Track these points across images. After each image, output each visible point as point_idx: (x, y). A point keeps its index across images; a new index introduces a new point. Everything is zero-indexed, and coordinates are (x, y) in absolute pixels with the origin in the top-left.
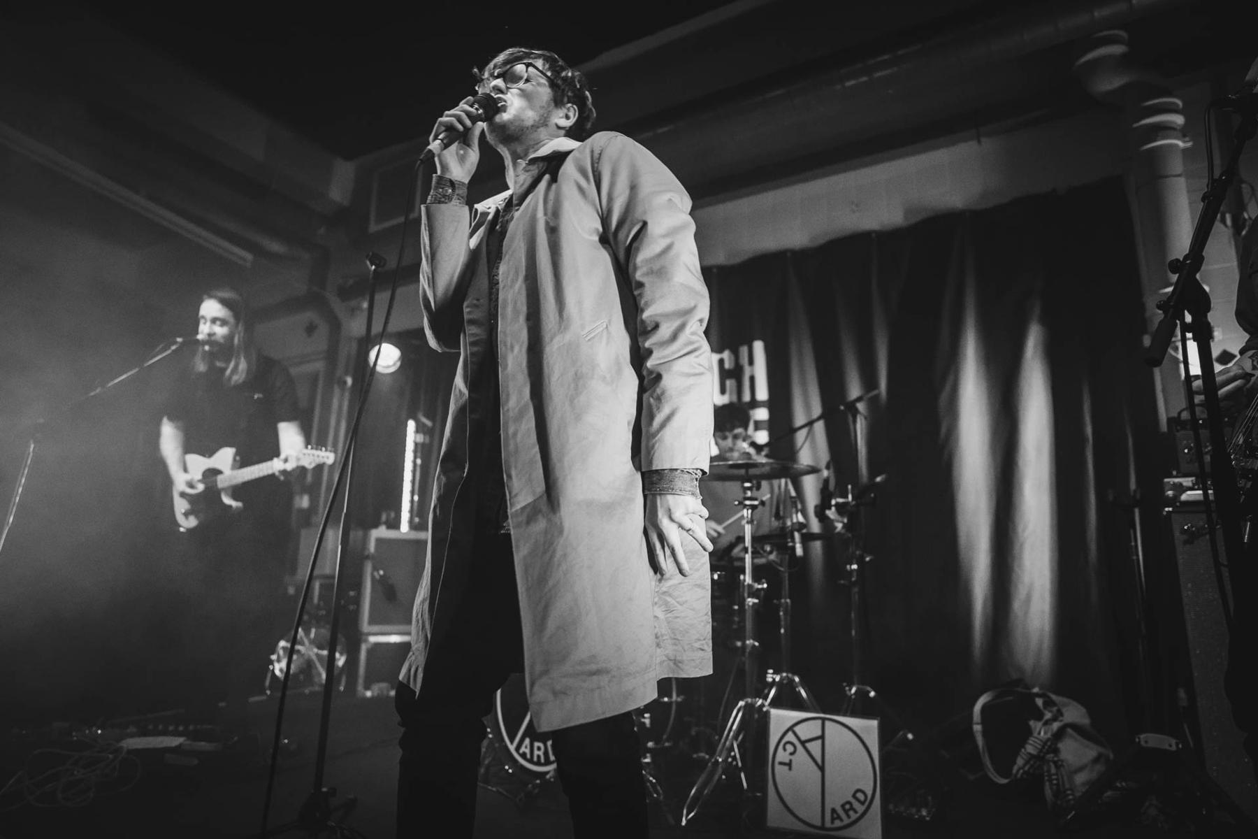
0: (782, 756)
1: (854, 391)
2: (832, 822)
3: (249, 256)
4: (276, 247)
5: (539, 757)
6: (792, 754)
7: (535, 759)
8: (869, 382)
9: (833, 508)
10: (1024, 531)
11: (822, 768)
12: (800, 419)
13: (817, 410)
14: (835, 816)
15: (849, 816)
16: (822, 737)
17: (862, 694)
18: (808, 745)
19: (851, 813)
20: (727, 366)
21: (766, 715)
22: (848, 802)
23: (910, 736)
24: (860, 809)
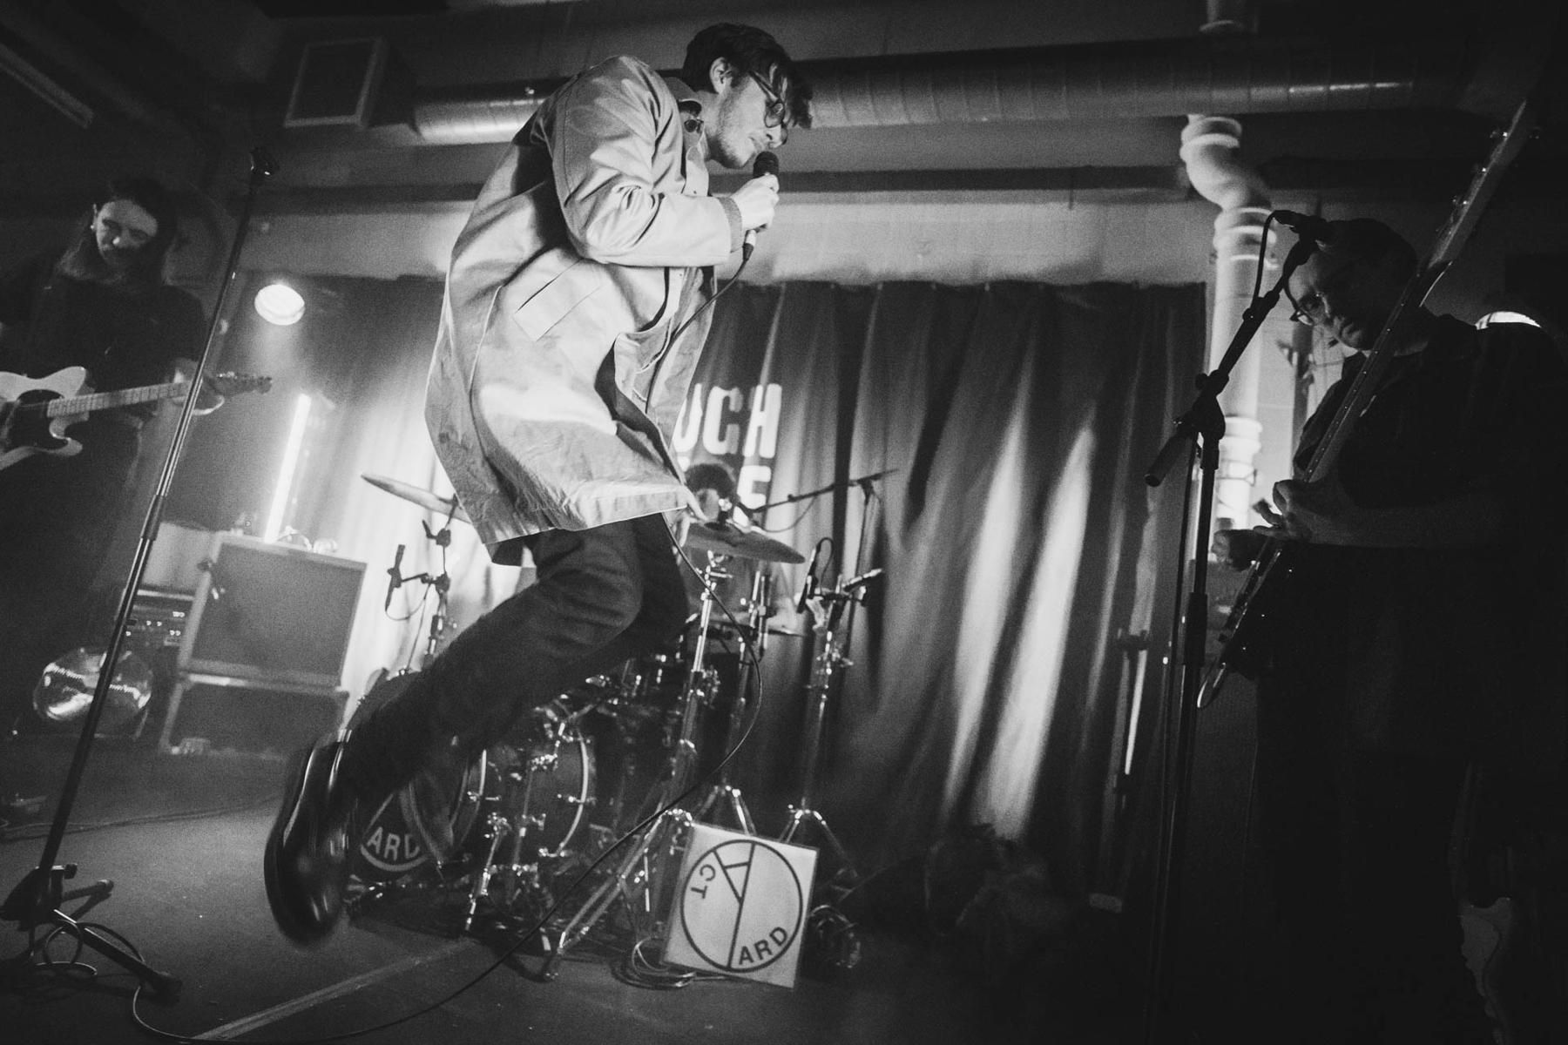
2: (741, 963)
5: (391, 852)
6: (709, 880)
7: (386, 855)
11: (741, 900)
13: (828, 479)
14: (746, 956)
15: (761, 958)
16: (748, 864)
17: (809, 821)
18: (729, 871)
19: (765, 954)
20: (732, 407)
21: (688, 831)
22: (764, 942)
24: (776, 949)
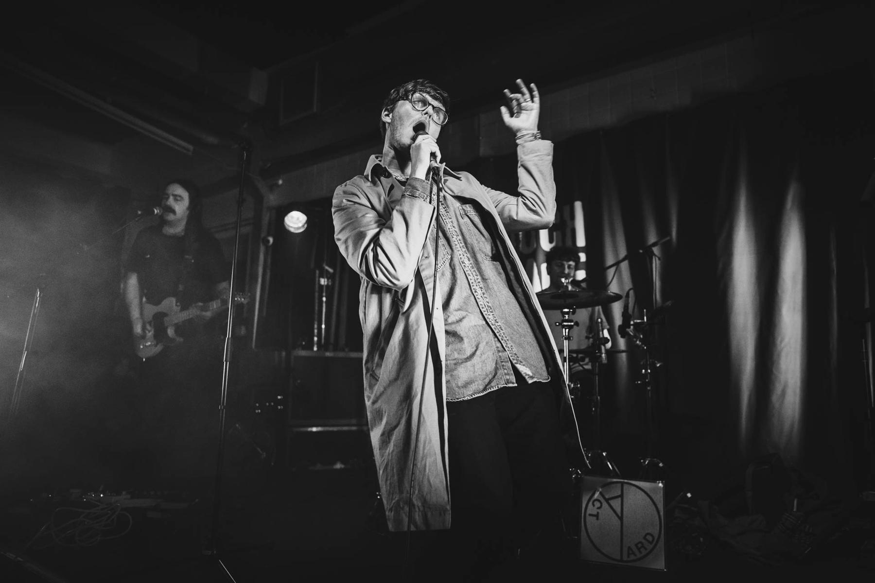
0: (592, 510)
1: (652, 238)
2: (628, 557)
3: (191, 147)
4: (211, 140)
6: (598, 508)
8: (663, 231)
9: (632, 327)
10: (781, 342)
11: (621, 518)
12: (610, 260)
13: (623, 253)
15: (640, 552)
16: (621, 496)
18: (611, 502)
22: (640, 542)
23: (689, 495)
